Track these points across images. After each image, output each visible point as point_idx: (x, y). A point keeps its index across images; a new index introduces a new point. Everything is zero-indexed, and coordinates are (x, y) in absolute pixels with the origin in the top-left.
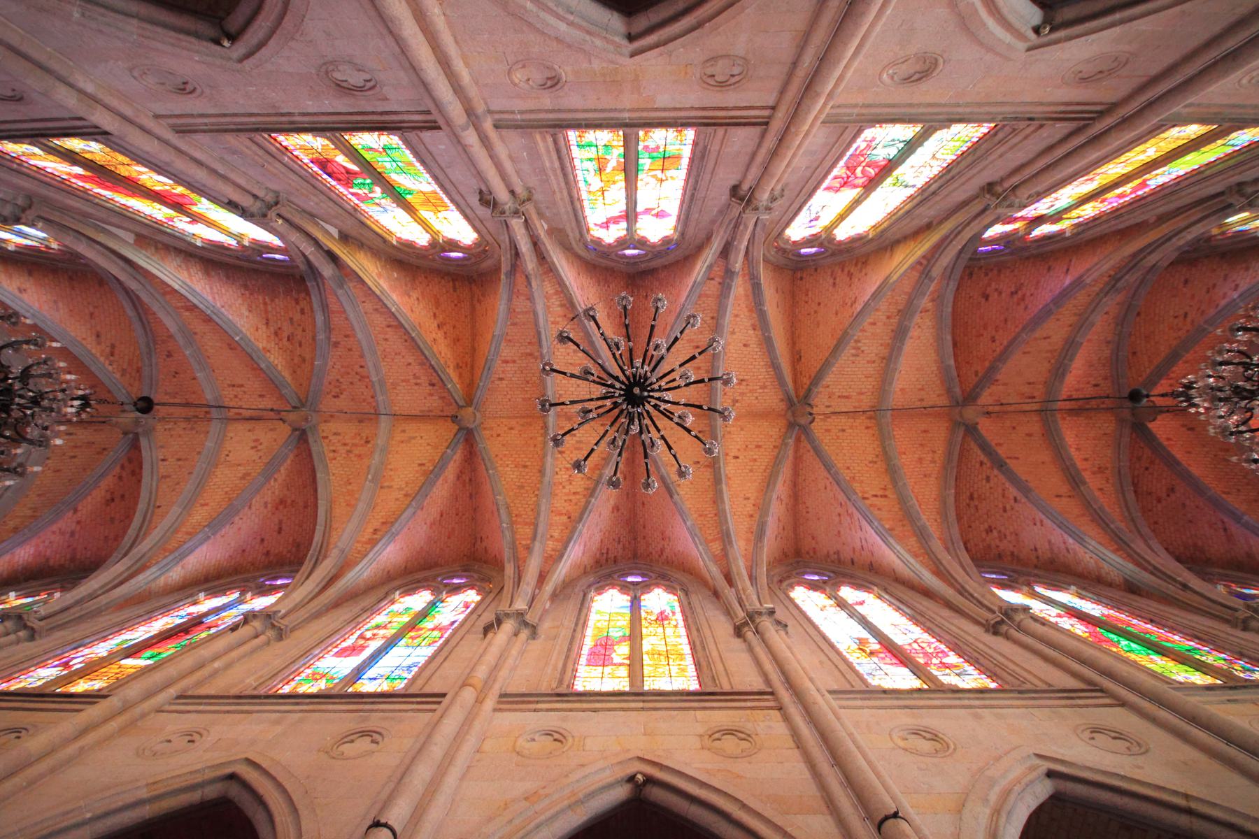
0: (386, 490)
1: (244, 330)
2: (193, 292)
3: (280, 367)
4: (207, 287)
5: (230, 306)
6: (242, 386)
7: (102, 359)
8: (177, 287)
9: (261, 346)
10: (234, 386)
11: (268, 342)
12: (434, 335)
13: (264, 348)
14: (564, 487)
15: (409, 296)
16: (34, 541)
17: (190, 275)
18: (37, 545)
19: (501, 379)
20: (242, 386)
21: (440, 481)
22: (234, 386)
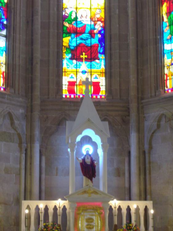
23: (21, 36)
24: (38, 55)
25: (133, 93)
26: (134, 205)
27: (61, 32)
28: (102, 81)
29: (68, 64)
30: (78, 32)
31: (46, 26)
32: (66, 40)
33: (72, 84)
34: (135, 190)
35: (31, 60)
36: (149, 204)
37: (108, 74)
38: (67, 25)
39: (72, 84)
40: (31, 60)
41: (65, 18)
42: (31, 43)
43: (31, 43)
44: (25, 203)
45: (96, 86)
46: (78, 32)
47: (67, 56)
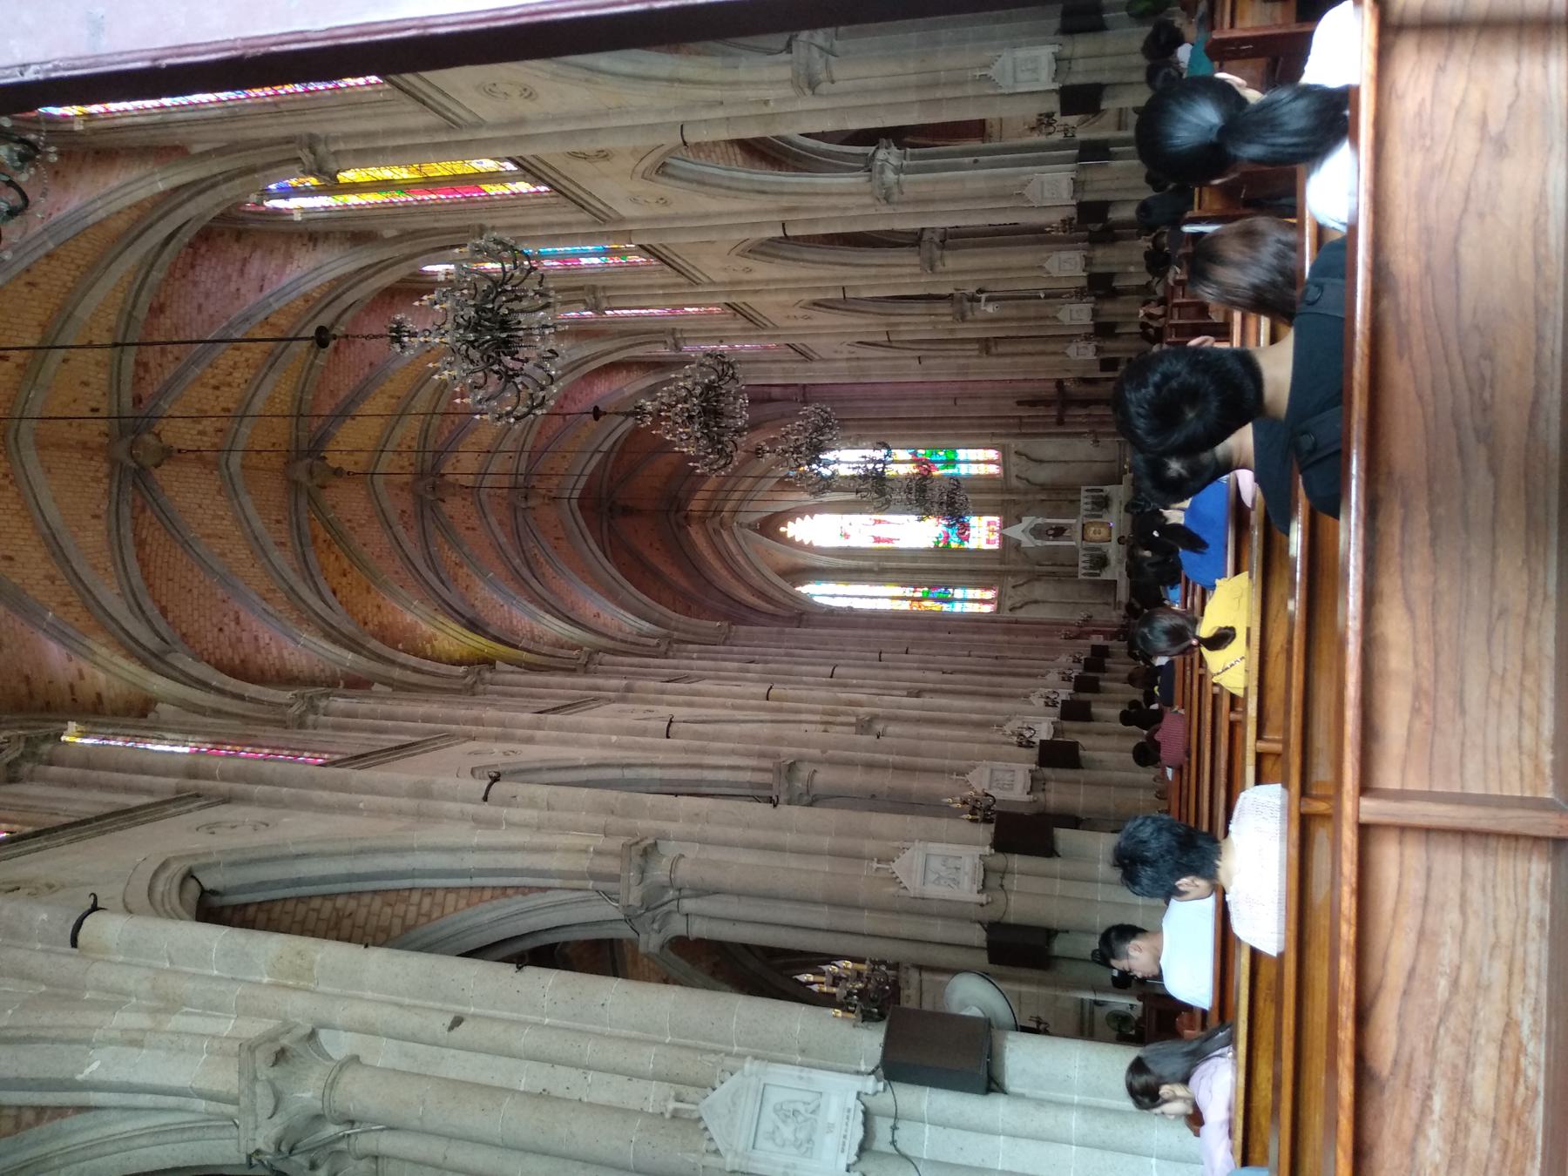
0: (398, 394)
1: (482, 584)
2: (532, 616)
3: (446, 547)
4: (515, 623)
5: (494, 607)
6: (468, 528)
7: (542, 560)
8: (548, 617)
9: (465, 569)
10: (474, 529)
11: (456, 574)
12: (344, 581)
13: (461, 567)
14: (247, 360)
15: (380, 624)
16: (595, 396)
17: (532, 631)
18: (592, 392)
19: (278, 522)
20: (468, 528)
21: (342, 395)
22: (474, 529)
23: (953, 578)
24: (967, 566)
25: (999, 497)
26: (1083, 500)
27: (947, 548)
28: (986, 519)
29: (972, 544)
30: (947, 537)
31: (943, 560)
32: (954, 545)
33: (988, 542)
34: (1074, 498)
35: (971, 572)
36: (1083, 488)
37: (980, 514)
38: (941, 545)
39: (988, 542)
40: (971, 572)
41: (936, 546)
42: (957, 572)
43: (957, 572)
44: (1081, 577)
45: (989, 524)
46: (947, 537)
47: (966, 545)
